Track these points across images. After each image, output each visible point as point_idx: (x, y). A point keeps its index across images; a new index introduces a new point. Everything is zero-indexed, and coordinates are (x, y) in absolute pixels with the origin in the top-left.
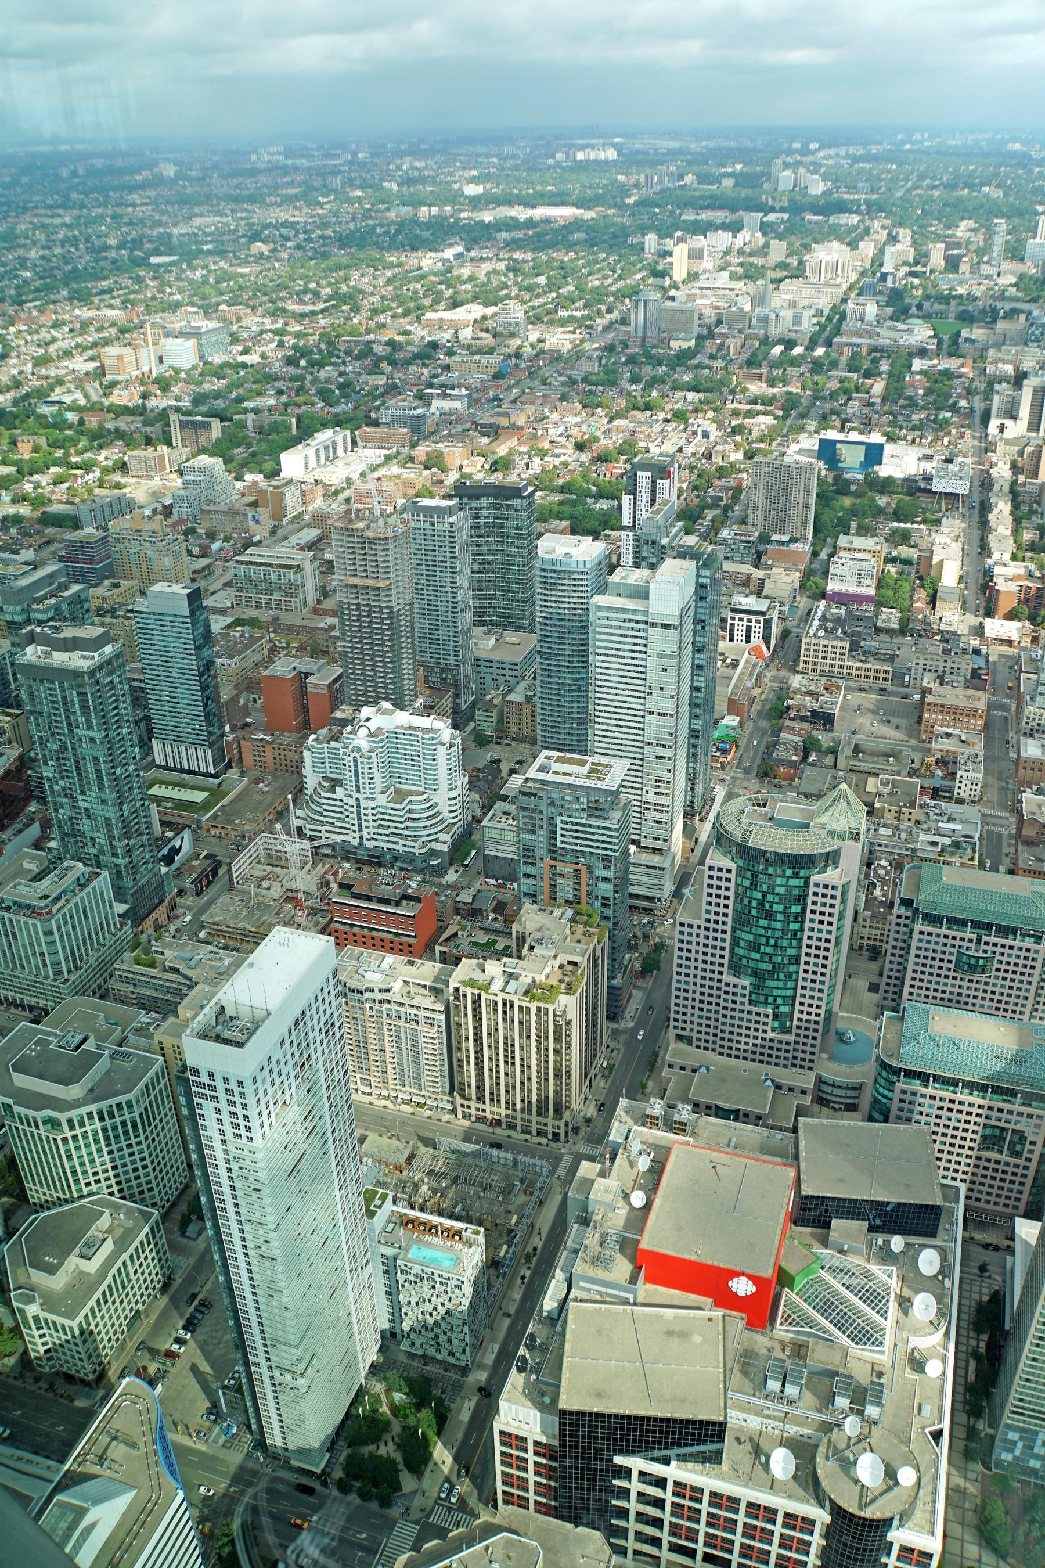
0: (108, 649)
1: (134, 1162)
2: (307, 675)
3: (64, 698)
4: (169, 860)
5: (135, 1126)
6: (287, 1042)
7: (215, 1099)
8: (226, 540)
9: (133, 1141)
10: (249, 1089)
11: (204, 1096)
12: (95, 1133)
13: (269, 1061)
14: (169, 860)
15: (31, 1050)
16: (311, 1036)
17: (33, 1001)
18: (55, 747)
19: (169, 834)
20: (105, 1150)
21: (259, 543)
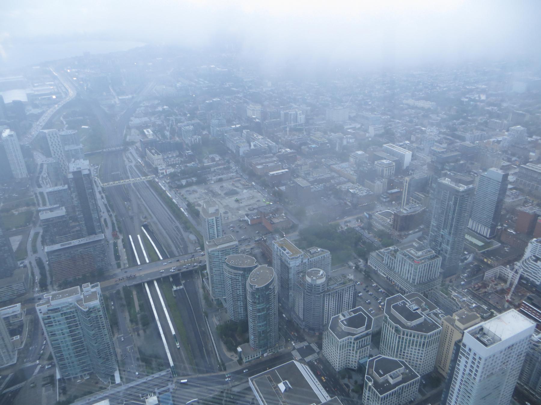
0: (471, 186)
1: (418, 356)
2: (539, 216)
3: (449, 197)
4: (462, 261)
5: (424, 345)
6: (503, 352)
7: (468, 358)
8: (519, 158)
9: (421, 349)
10: (482, 362)
11: (464, 355)
12: (410, 341)
13: (494, 356)
14: (462, 261)
15: (399, 303)
16: (512, 354)
17: (402, 287)
18: (440, 211)
19: (466, 253)
20: (411, 347)
21: (531, 162)
